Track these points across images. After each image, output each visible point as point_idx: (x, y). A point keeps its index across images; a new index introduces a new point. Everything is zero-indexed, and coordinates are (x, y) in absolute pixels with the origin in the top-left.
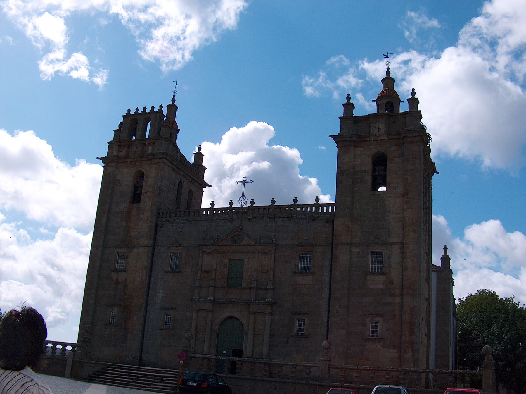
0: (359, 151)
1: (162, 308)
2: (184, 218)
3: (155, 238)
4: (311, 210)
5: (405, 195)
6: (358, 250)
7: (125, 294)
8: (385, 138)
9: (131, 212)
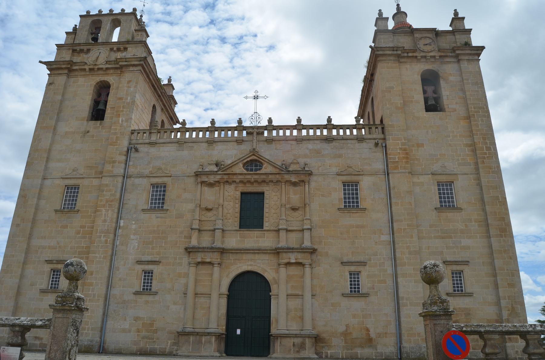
4: (351, 132)
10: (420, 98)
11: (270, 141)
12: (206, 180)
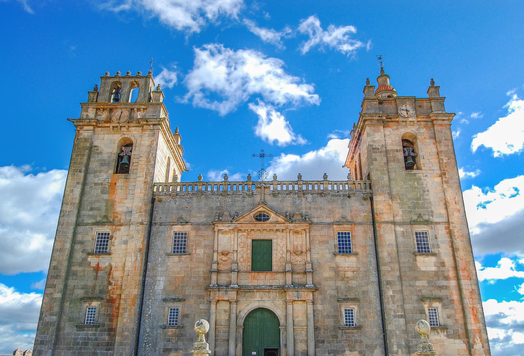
0: (388, 131)
3: (151, 215)
6: (402, 229)
7: (110, 284)
8: (413, 120)
10: (401, 156)
11: (275, 194)
12: (222, 228)
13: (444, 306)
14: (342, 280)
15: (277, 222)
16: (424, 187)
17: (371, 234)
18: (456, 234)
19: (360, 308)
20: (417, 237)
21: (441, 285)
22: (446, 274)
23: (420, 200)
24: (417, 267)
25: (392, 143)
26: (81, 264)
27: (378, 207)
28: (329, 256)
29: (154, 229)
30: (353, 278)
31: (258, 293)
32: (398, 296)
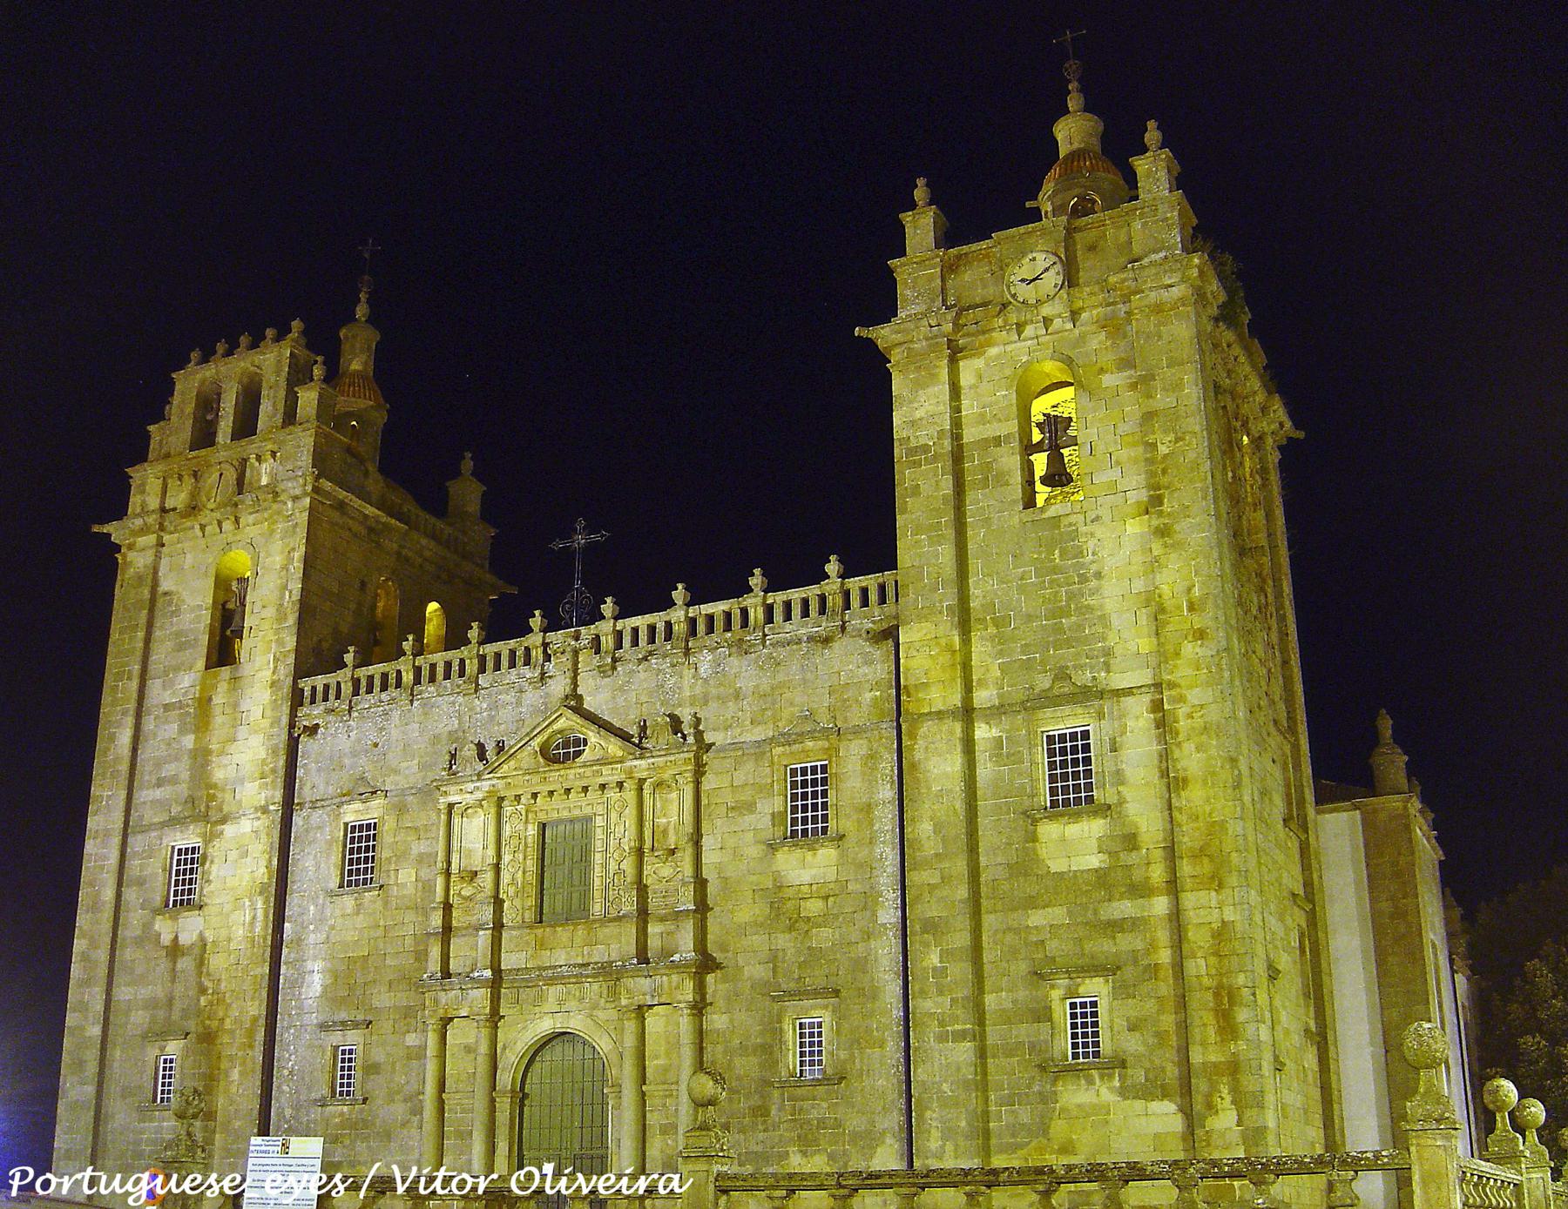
1: (324, 1027)
2: (384, 696)
5: (1154, 503)
6: (995, 732)
9: (210, 699)
13: (1122, 991)
14: (791, 929)
15: (604, 761)
16: (1082, 565)
17: (888, 764)
18: (1183, 724)
19: (840, 1016)
20: (1051, 753)
21: (1117, 915)
22: (1137, 875)
23: (1069, 616)
24: (1037, 860)
25: (982, 415)
26: (139, 942)
27: (914, 663)
28: (755, 851)
29: (297, 820)
30: (825, 919)
31: (552, 989)
32: (960, 970)
